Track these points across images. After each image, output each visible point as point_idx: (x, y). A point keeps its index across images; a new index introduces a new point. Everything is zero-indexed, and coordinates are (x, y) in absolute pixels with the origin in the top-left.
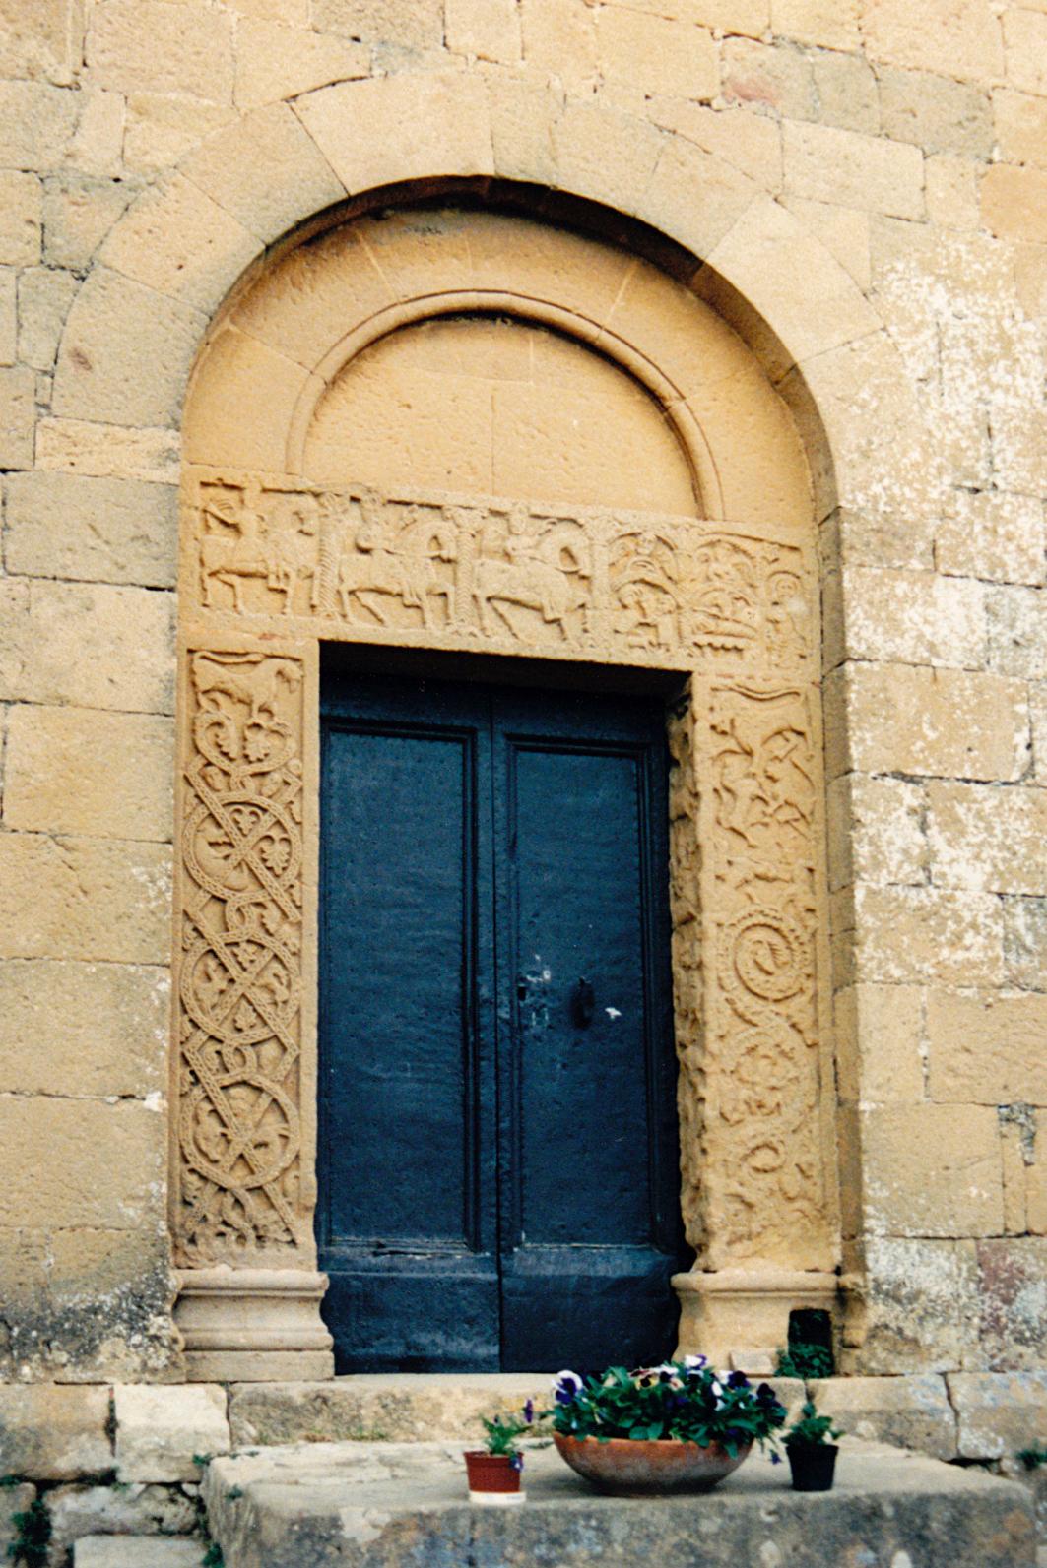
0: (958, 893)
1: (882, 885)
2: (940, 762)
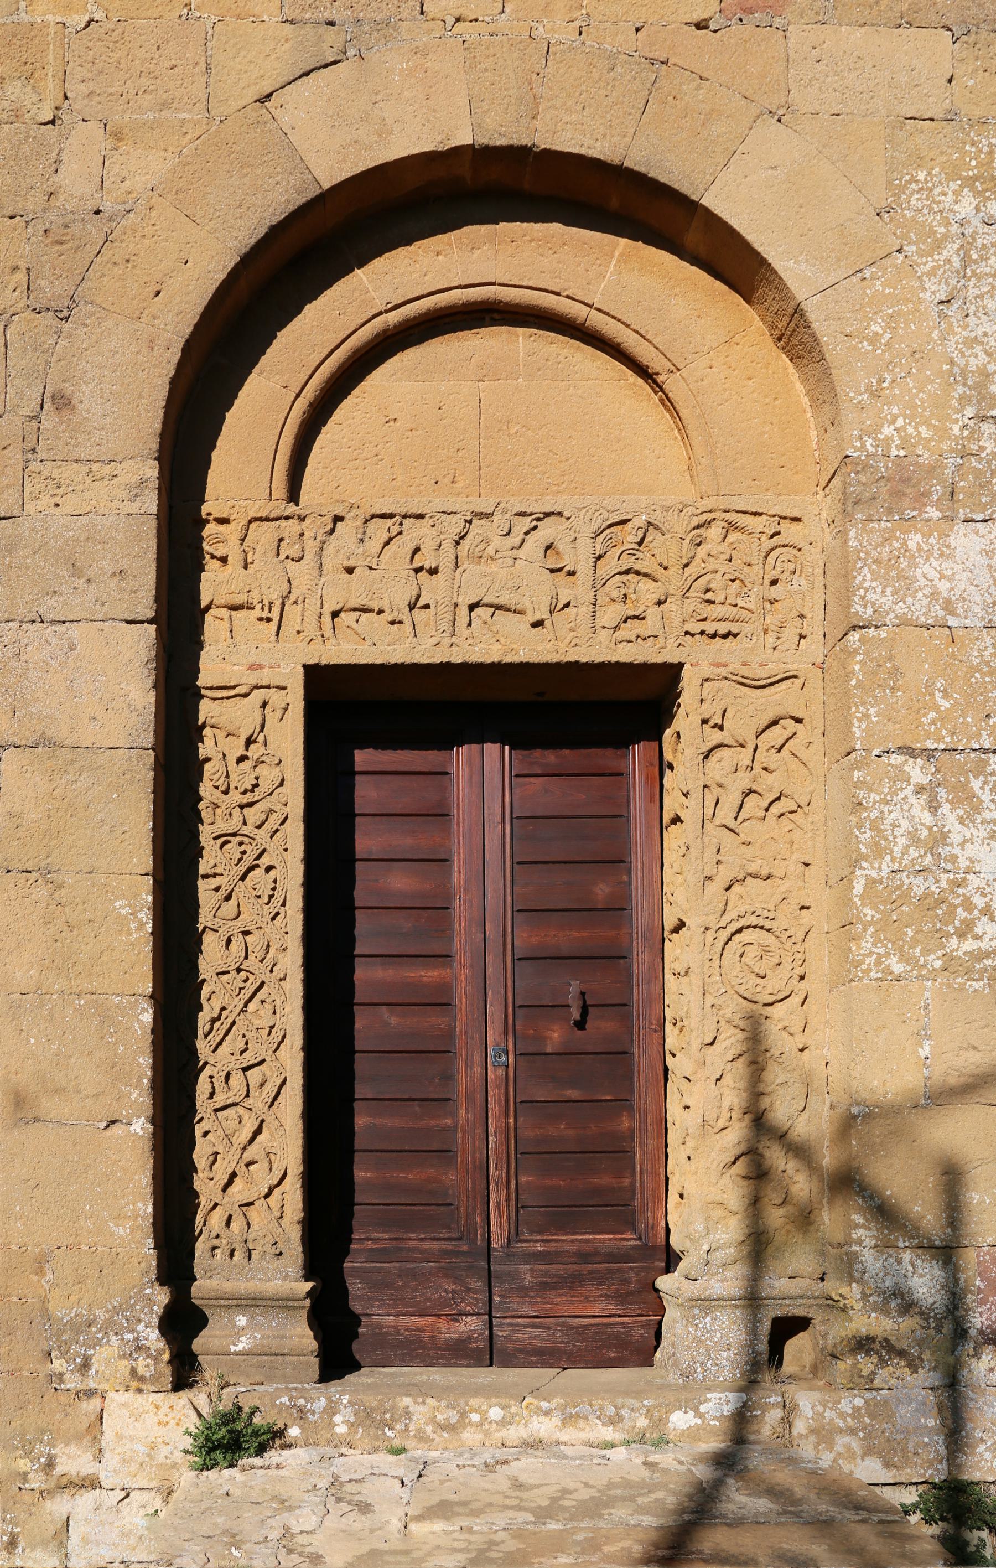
0: (970, 877)
1: (885, 871)
2: (953, 734)
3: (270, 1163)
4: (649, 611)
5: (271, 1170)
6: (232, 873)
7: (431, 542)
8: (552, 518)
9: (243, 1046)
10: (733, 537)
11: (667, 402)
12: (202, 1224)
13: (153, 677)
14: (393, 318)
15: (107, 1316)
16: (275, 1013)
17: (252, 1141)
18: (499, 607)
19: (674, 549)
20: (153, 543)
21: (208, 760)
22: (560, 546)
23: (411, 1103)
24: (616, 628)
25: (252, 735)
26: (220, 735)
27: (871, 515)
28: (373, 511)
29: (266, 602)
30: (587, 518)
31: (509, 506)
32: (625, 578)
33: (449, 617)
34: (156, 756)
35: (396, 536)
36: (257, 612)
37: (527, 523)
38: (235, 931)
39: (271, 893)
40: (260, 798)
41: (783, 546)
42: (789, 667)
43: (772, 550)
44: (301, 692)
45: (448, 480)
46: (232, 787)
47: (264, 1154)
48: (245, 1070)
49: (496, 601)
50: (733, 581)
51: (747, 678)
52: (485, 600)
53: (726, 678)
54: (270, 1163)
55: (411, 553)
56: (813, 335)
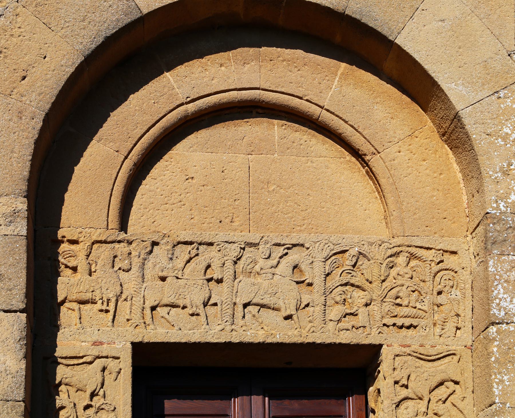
4: (360, 310)
7: (218, 262)
8: (297, 248)
10: (413, 263)
11: (371, 174)
13: (24, 350)
14: (191, 108)
18: (263, 306)
19: (376, 271)
20: (24, 256)
22: (303, 267)
24: (339, 321)
26: (72, 390)
27: (504, 251)
28: (179, 239)
29: (105, 299)
30: (320, 248)
31: (269, 239)
32: (344, 288)
33: (230, 311)
34: (25, 406)
35: (194, 257)
36: (99, 306)
37: (281, 250)
41: (446, 270)
42: (450, 348)
43: (438, 272)
44: (129, 361)
45: (228, 220)
49: (261, 302)
50: (413, 292)
51: (423, 355)
52: (254, 301)
53: (410, 355)
55: (204, 268)
56: (466, 134)
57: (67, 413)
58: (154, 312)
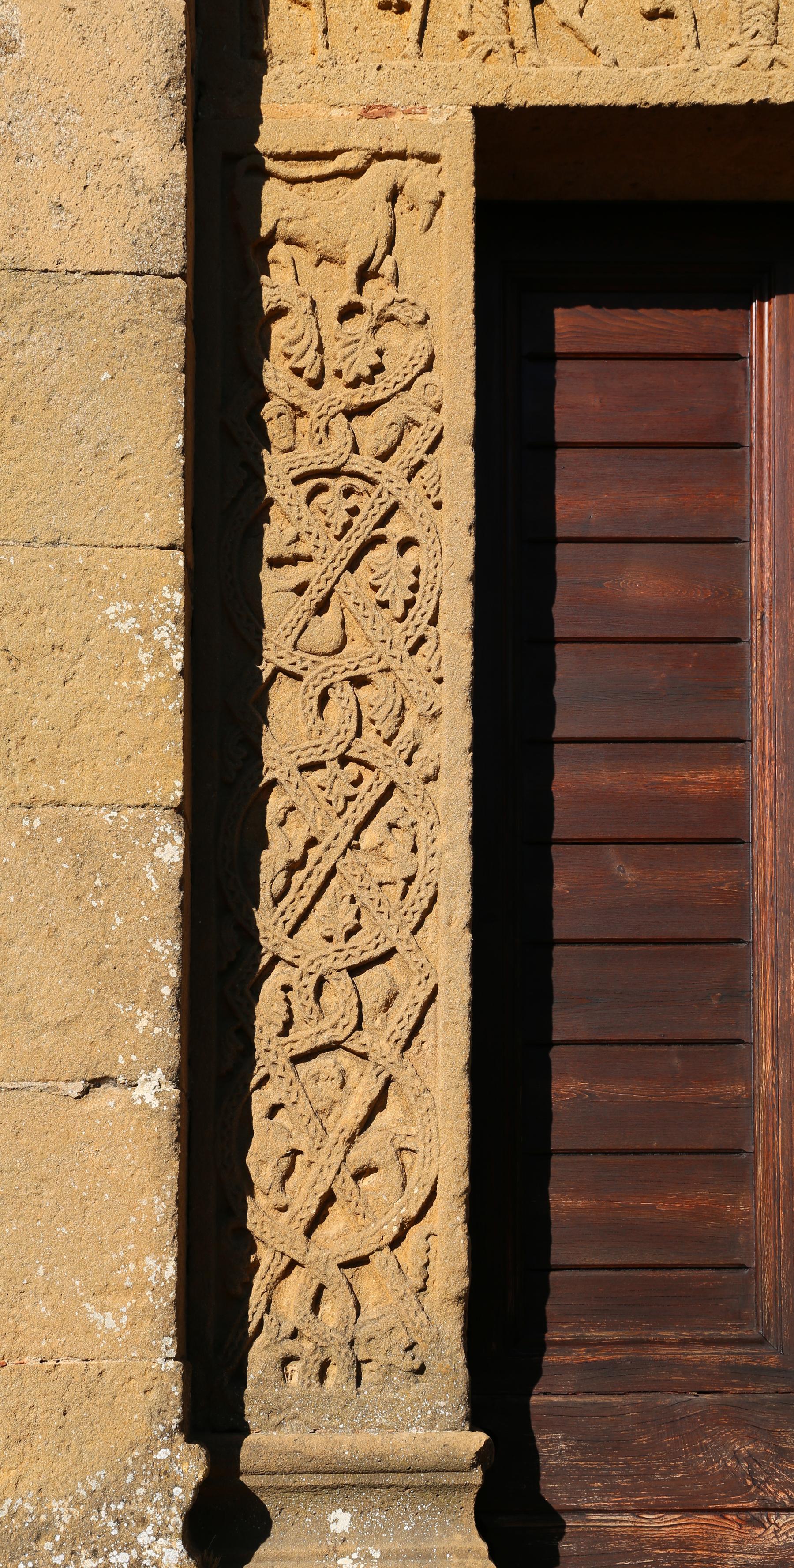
3: (403, 1171)
5: (404, 1185)
6: (330, 555)
9: (349, 919)
12: (262, 1307)
15: (77, 1513)
16: (414, 850)
17: (365, 1124)
21: (280, 312)
23: (664, 1049)
25: (370, 260)
26: (305, 259)
38: (338, 677)
39: (410, 595)
40: (387, 393)
46: (329, 372)
47: (391, 1151)
48: (355, 971)
54: (403, 1171)
57: (294, 327)
58: (537, 9)
